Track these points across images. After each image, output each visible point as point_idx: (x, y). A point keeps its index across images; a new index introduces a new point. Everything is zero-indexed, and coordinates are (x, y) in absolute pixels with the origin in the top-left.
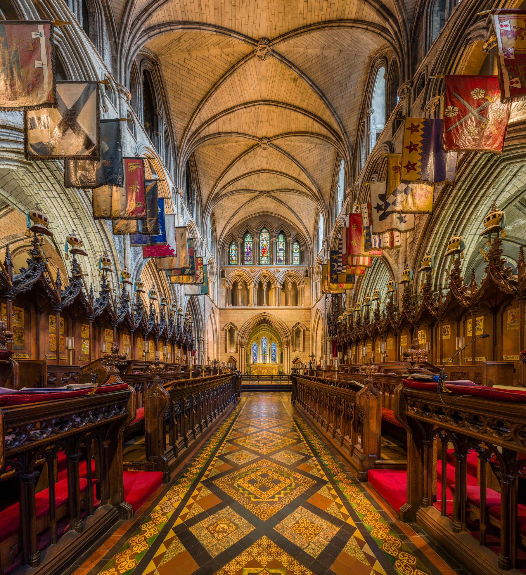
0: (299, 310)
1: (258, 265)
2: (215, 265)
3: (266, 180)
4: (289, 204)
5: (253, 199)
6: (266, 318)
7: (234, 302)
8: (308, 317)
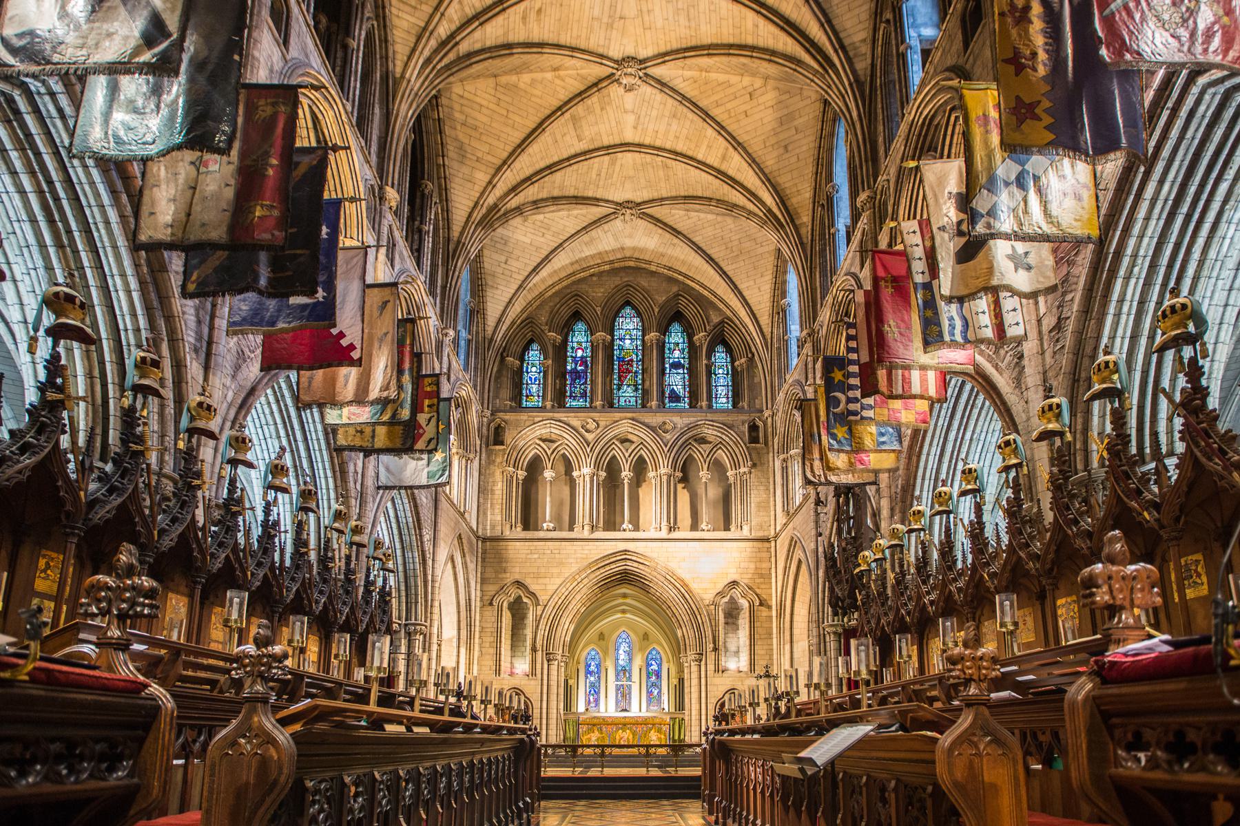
3: (631, 173)
5: (595, 222)
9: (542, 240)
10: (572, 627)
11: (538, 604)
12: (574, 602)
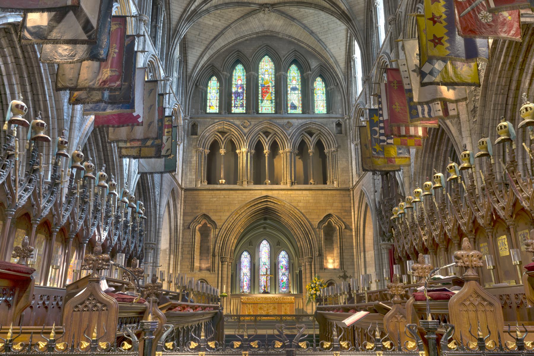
0: (330, 192)
1: (256, 115)
2: (182, 115)
4: (305, 22)
6: (270, 205)
7: (211, 179)
8: (347, 205)
9: (219, 23)
10: (236, 241)
11: (216, 228)
12: (237, 227)
